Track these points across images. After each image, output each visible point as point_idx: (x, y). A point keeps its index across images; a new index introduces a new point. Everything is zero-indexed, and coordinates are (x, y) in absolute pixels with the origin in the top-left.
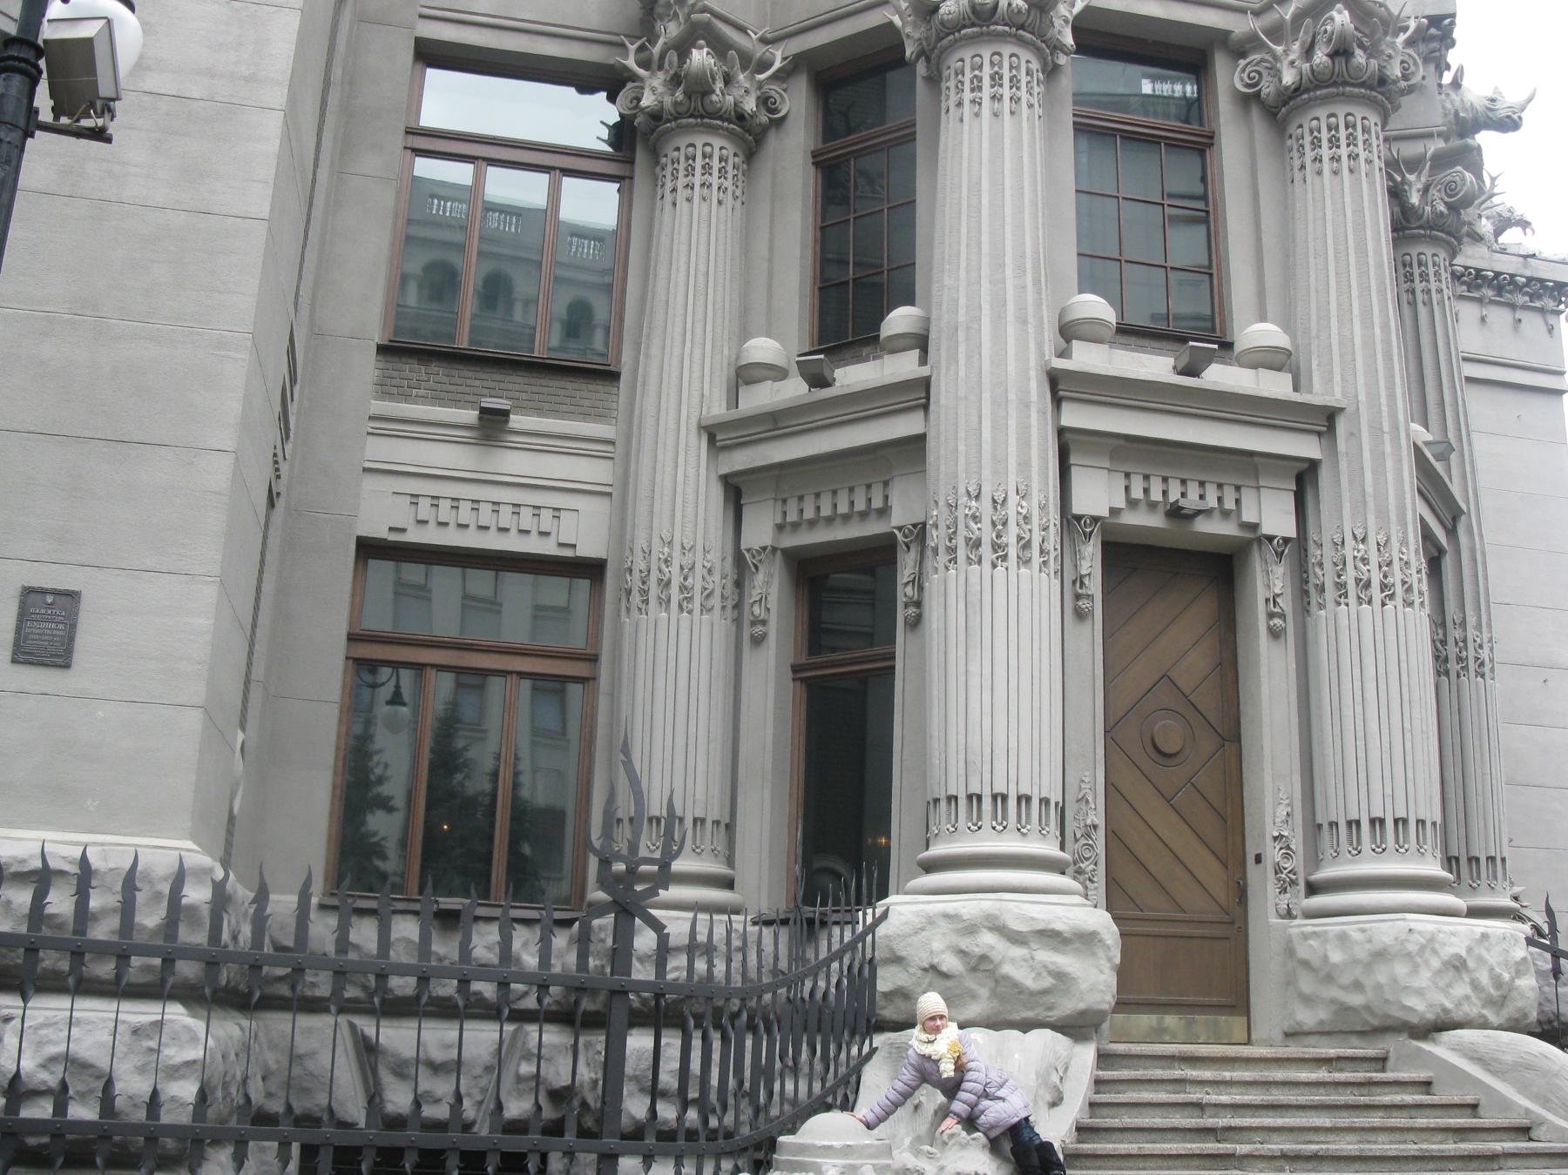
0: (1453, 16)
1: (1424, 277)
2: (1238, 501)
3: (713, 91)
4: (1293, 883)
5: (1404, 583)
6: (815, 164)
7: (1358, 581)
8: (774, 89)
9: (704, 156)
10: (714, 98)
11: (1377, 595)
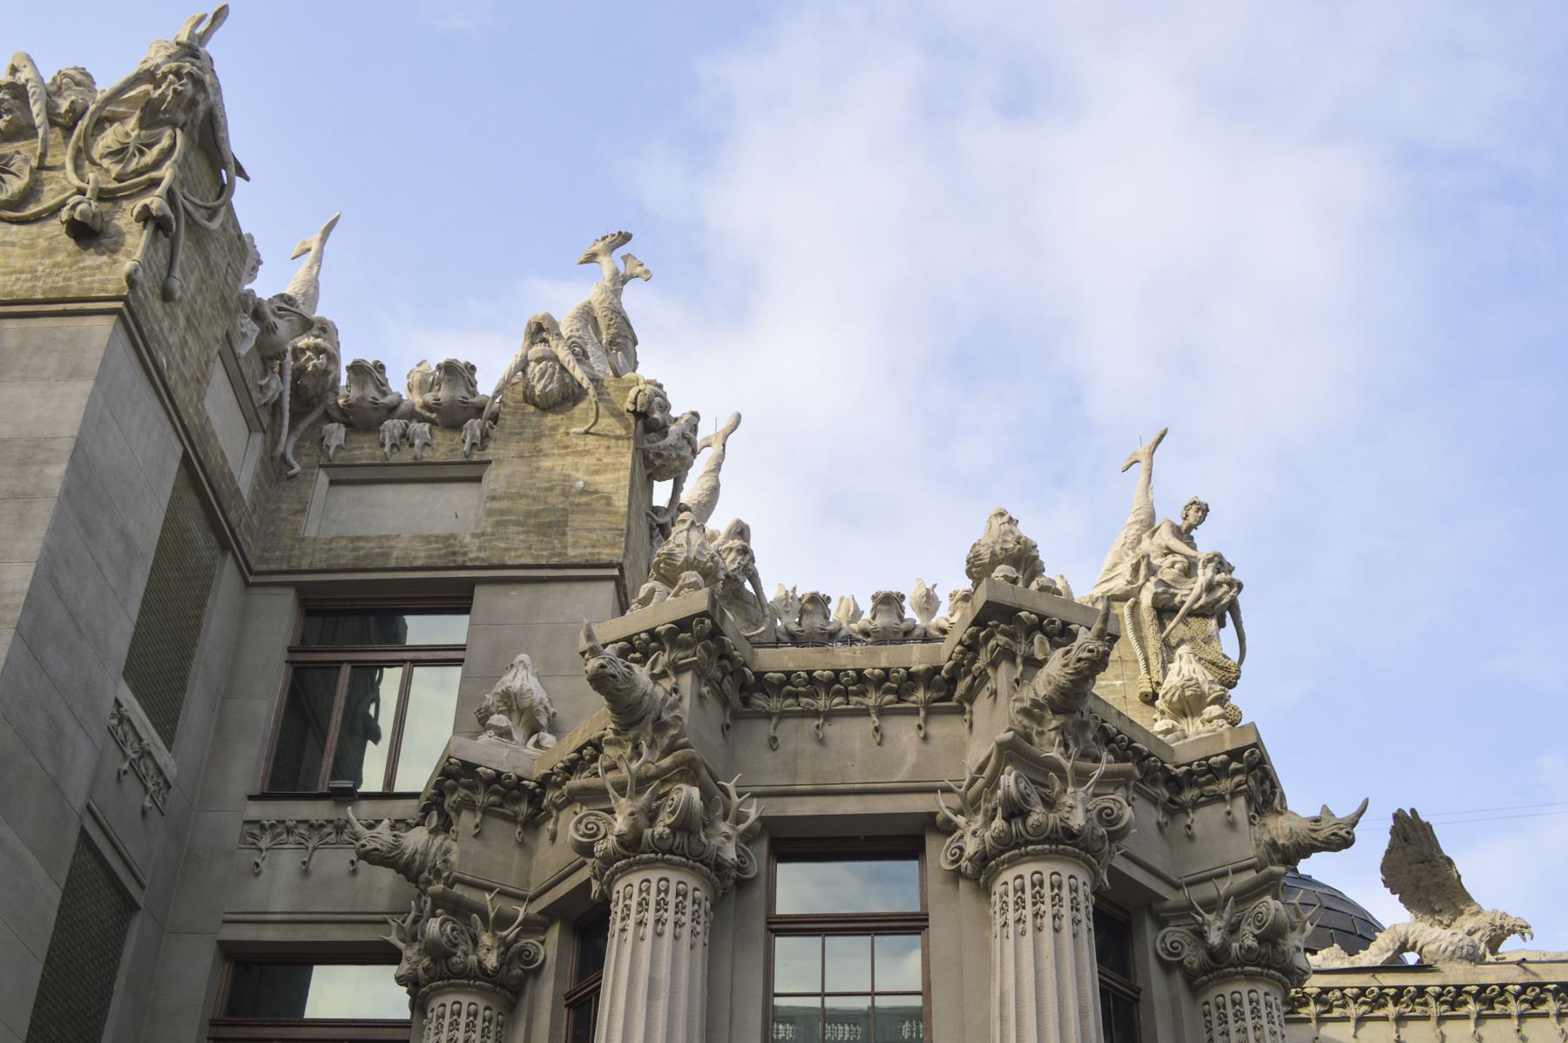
1: (1239, 1016)
9: (452, 1014)
10: (455, 959)
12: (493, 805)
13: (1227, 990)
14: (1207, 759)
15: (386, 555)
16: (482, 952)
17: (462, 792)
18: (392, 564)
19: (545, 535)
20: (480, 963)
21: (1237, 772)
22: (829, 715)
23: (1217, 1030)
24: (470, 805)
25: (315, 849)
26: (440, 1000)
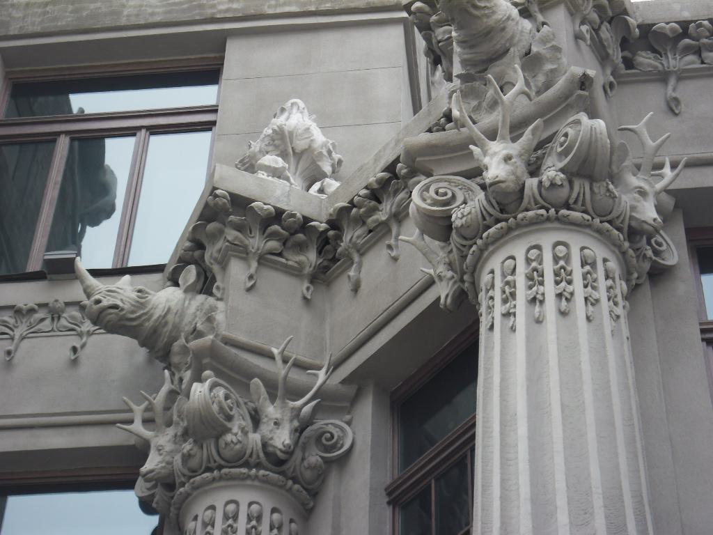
3: (228, 430)
6: (393, 503)
8: (330, 424)
9: (226, 517)
10: (229, 437)
15: (116, 13)
16: (266, 428)
17: (231, 234)
18: (123, 21)
20: (265, 445)
24: (242, 252)
25: (23, 338)
26: (208, 501)
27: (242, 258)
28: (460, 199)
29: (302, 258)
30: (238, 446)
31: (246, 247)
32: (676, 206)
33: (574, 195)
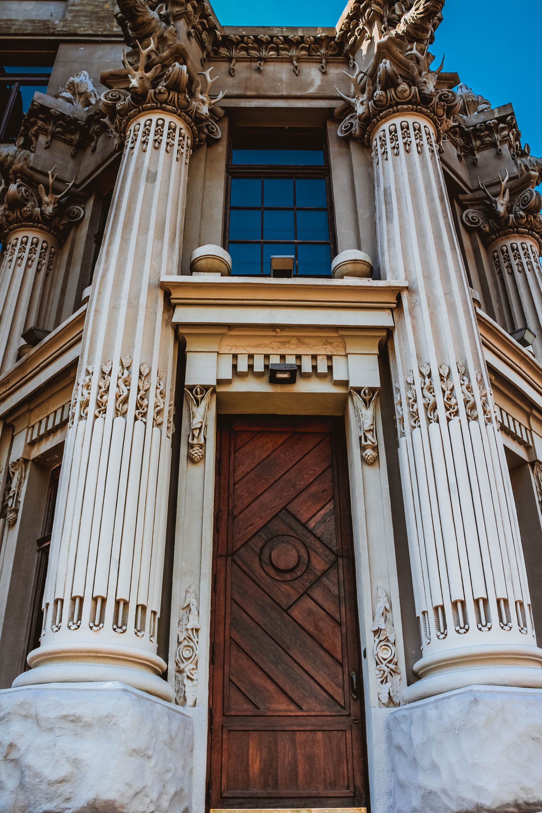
0: (513, 114)
2: (330, 368)
4: (393, 672)
5: (466, 402)
7: (426, 407)
10: (25, 209)
11: (441, 412)
12: (58, 132)
13: (508, 243)
14: (485, 122)
17: (40, 123)
19: (101, 22)
21: (503, 129)
22: (265, 60)
23: (504, 265)
24: (45, 132)
27: (44, 134)
28: (123, 98)
29: (73, 137)
30: (29, 213)
31: (47, 129)
32: (225, 115)
33: (170, 98)
